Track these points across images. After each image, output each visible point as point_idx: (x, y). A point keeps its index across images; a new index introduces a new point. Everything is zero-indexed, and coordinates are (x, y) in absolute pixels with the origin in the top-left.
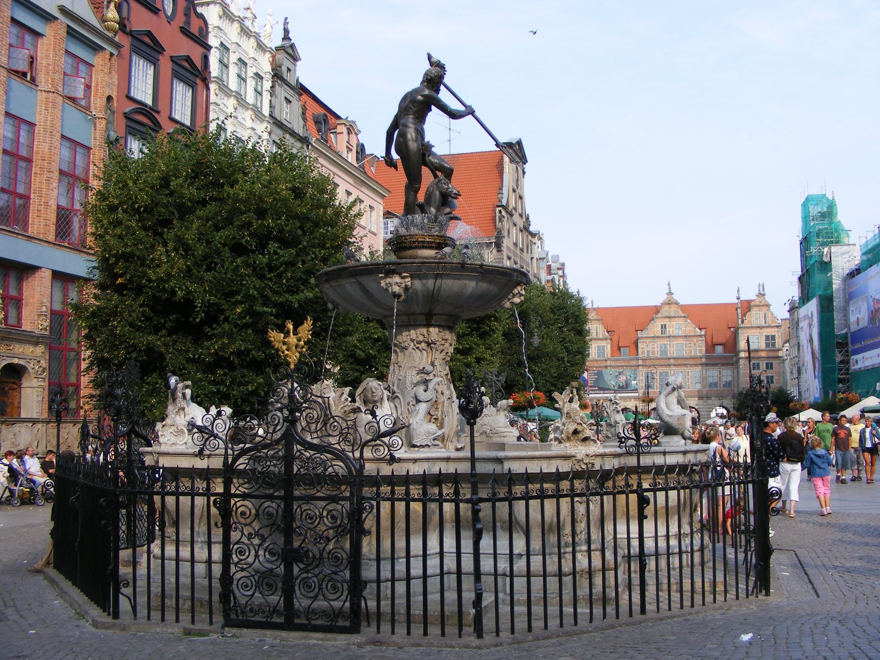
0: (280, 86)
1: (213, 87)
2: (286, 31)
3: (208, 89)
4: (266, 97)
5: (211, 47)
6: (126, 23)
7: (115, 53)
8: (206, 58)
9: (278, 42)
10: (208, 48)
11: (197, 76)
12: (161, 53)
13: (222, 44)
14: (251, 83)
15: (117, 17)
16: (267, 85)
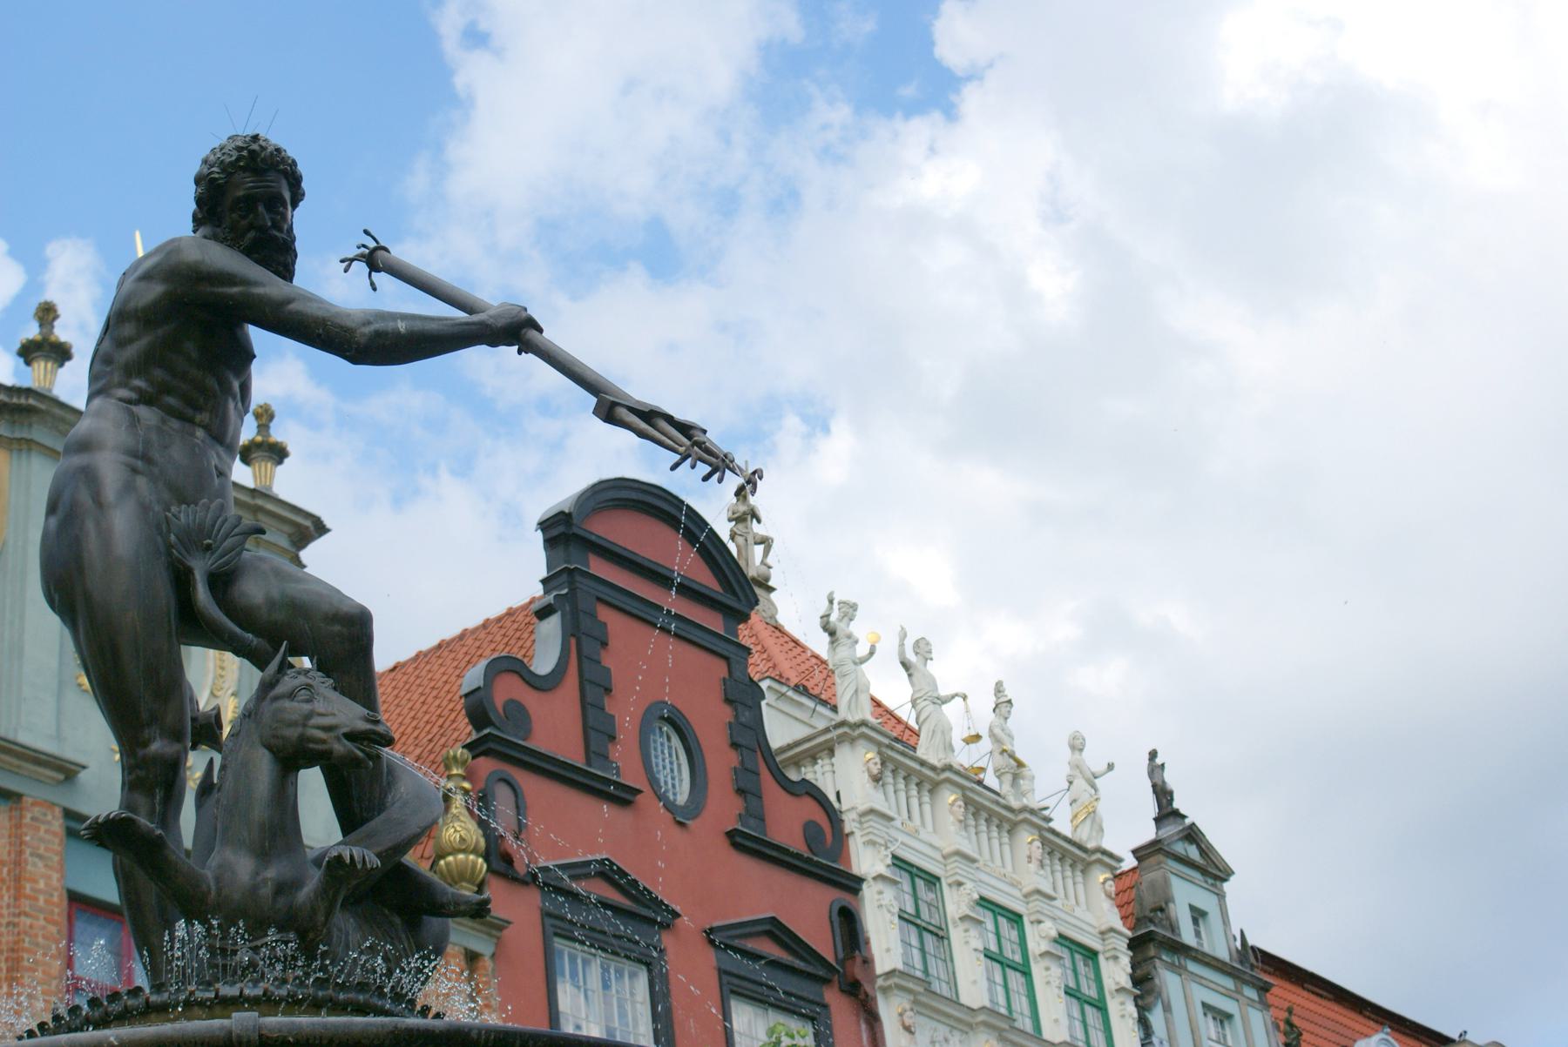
0: (1178, 969)
1: (889, 1010)
2: (1163, 794)
3: (873, 1019)
4: (1122, 1013)
5: (860, 880)
6: (511, 843)
7: (484, 947)
8: (849, 924)
9: (1147, 832)
10: (853, 884)
11: (825, 981)
12: (665, 926)
13: (899, 862)
14: (1049, 980)
15: (475, 835)
16: (1117, 972)
